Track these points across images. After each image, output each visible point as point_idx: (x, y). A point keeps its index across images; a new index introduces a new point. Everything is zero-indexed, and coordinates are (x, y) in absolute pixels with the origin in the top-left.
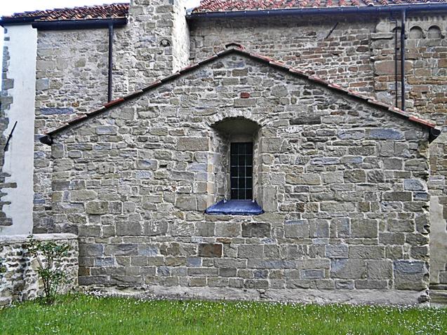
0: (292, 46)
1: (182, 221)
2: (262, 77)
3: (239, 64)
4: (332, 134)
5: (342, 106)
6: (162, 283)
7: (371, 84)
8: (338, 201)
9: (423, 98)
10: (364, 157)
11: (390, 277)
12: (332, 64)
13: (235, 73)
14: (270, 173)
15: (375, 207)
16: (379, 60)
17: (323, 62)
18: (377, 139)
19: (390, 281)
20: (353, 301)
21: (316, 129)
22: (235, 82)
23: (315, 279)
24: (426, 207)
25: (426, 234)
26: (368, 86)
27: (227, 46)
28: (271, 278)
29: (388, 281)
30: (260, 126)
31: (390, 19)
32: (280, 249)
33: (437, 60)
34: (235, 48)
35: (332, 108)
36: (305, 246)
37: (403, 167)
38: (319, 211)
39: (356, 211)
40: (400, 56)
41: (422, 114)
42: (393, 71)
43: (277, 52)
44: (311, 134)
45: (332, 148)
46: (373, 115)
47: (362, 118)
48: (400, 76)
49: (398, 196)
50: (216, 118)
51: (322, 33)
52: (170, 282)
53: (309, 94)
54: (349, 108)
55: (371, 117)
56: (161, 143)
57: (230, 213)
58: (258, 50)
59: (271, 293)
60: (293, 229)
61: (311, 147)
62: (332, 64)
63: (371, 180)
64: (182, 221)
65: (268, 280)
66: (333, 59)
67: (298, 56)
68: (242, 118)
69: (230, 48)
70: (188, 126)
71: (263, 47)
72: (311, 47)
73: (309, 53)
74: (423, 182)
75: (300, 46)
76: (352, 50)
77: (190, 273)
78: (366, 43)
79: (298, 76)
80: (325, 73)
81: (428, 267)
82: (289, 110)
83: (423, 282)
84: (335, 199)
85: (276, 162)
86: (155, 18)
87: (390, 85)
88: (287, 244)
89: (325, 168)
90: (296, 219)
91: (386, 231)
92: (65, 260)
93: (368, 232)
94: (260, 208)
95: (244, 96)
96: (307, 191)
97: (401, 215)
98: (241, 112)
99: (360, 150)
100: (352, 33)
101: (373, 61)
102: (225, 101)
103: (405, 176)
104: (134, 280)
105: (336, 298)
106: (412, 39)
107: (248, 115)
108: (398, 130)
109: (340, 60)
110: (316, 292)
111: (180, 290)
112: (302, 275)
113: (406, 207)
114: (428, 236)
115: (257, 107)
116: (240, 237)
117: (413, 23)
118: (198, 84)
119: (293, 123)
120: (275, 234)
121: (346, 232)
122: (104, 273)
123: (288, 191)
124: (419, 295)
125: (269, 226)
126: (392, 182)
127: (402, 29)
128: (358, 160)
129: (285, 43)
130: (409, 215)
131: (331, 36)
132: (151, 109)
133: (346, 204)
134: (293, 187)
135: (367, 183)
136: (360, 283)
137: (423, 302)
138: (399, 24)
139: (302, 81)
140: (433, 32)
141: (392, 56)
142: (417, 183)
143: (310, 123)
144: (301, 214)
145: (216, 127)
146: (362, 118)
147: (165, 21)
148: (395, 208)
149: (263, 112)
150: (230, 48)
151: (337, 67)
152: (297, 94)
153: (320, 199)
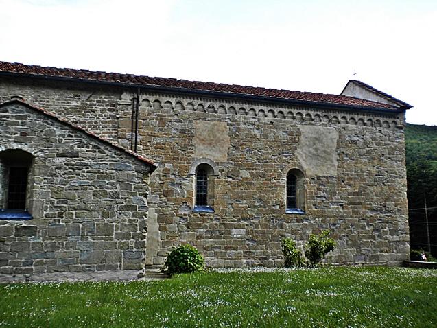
0: (62, 102)
2: (37, 122)
3: (21, 112)
5: (94, 147)
7: (116, 133)
8: (88, 211)
9: (148, 145)
10: (107, 182)
11: (120, 262)
13: (17, 117)
14: (39, 188)
15: (113, 215)
16: (122, 118)
17: (84, 115)
18: (116, 170)
19: (121, 265)
20: (94, 279)
21: (75, 161)
22: (16, 124)
23: (68, 265)
24: (146, 215)
26: (114, 135)
27: (12, 97)
28: (35, 266)
29: (119, 264)
30: (34, 157)
31: (130, 93)
32: (44, 245)
34: (18, 99)
35: (88, 147)
36: (63, 243)
37: (133, 189)
38: (74, 218)
39: (100, 218)
40: (136, 116)
41: (147, 155)
42: (131, 126)
43: (51, 105)
44: (71, 164)
45: (85, 174)
46: (115, 154)
47: (107, 156)
48: (135, 129)
49: (128, 208)
51: (84, 97)
53: (72, 136)
54: (99, 148)
55: (113, 155)
57: (6, 219)
58: (37, 103)
63: (112, 197)
65: (33, 267)
66: (92, 114)
67: (66, 110)
68: (21, 150)
69: (14, 99)
71: (41, 101)
72: (76, 104)
73: (75, 109)
74: (144, 199)
75: (68, 103)
78: (114, 106)
79: (64, 123)
80: (85, 123)
81: (145, 254)
82: (56, 146)
83: (141, 264)
84: (85, 210)
85: (44, 183)
87: (128, 135)
88: (49, 241)
89: (80, 188)
90: (57, 223)
91: (119, 231)
94: (31, 215)
95: (23, 134)
96: (66, 204)
97: (130, 220)
98: (19, 146)
100: (105, 98)
101: (118, 118)
102: (7, 137)
103: (134, 195)
105: (81, 278)
106: (144, 107)
107: (26, 148)
108: (131, 165)
109: (96, 116)
110: (69, 274)
112: (59, 263)
113: (133, 216)
114: (146, 234)
115: (33, 143)
117: (145, 97)
119: (59, 156)
120: (41, 234)
121: (92, 232)
123: (52, 203)
124: (138, 273)
125: (36, 228)
126: (125, 199)
127: (138, 100)
128: (103, 183)
129: (57, 100)
130: (135, 220)
131: (90, 99)
133: (93, 213)
134: (56, 200)
135: (108, 199)
136: (100, 267)
137: (141, 277)
138: (136, 96)
139: (67, 128)
140: (157, 104)
141: (130, 117)
142: (141, 200)
143: (71, 157)
144: (61, 220)
146: (107, 156)
148: (126, 215)
149: (37, 147)
150: (14, 99)
151: (93, 120)
152: (63, 136)
153: (76, 210)
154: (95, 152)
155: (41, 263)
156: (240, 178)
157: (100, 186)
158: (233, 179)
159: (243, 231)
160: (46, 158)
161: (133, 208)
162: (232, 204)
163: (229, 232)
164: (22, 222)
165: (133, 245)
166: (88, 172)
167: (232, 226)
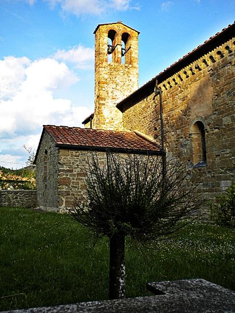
156: (224, 127)
158: (218, 128)
159: (229, 183)
162: (219, 155)
163: (219, 185)
167: (220, 178)
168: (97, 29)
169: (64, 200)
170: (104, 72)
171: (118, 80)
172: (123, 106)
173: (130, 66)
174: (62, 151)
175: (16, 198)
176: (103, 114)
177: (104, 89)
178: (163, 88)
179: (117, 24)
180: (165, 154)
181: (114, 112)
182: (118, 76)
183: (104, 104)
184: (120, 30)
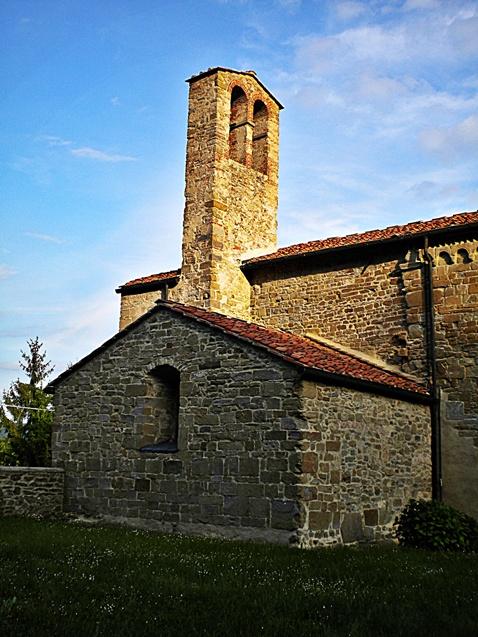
1: (125, 459)
3: (167, 318)
4: (228, 376)
6: (111, 513)
11: (268, 515)
12: (369, 299)
13: (165, 326)
17: (360, 298)
21: (217, 373)
22: (163, 334)
23: (211, 515)
25: (300, 474)
33: (466, 285)
35: (230, 352)
37: (281, 406)
39: (244, 450)
41: (453, 345)
45: (227, 389)
46: (260, 357)
50: (151, 367)
52: (116, 513)
54: (242, 352)
56: (116, 391)
59: (180, 526)
60: (197, 466)
61: (213, 389)
62: (369, 299)
64: (125, 459)
70: (132, 375)
76: (385, 284)
77: (130, 505)
86: (199, 274)
88: (193, 481)
92: (41, 489)
93: (250, 468)
99: (248, 390)
101: (405, 293)
104: (94, 509)
107: (172, 363)
111: (122, 520)
113: (282, 447)
116: (161, 473)
118: (140, 337)
122: (77, 502)
124: (290, 535)
128: (246, 401)
129: (327, 283)
132: (110, 361)
134: (199, 427)
137: (294, 542)
142: (292, 422)
143: (213, 368)
145: (152, 373)
147: (206, 277)
151: (373, 302)
153: (219, 439)
154: (237, 357)
155: (186, 510)
157: (243, 405)
160: (190, 371)
161: (282, 436)
164: (170, 454)
165: (283, 492)
166: (231, 386)
168: (203, 75)
169: (308, 512)
170: (222, 181)
171: (246, 204)
172: (255, 271)
173: (266, 177)
174: (306, 386)
175: (17, 491)
176: (218, 283)
177: (220, 222)
178: (438, 259)
179: (247, 77)
180: (439, 400)
181: (236, 281)
182: (245, 198)
183: (220, 258)
184: (252, 92)
